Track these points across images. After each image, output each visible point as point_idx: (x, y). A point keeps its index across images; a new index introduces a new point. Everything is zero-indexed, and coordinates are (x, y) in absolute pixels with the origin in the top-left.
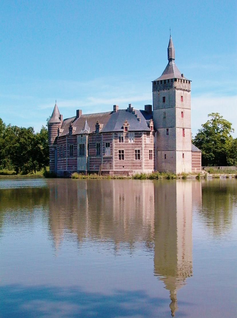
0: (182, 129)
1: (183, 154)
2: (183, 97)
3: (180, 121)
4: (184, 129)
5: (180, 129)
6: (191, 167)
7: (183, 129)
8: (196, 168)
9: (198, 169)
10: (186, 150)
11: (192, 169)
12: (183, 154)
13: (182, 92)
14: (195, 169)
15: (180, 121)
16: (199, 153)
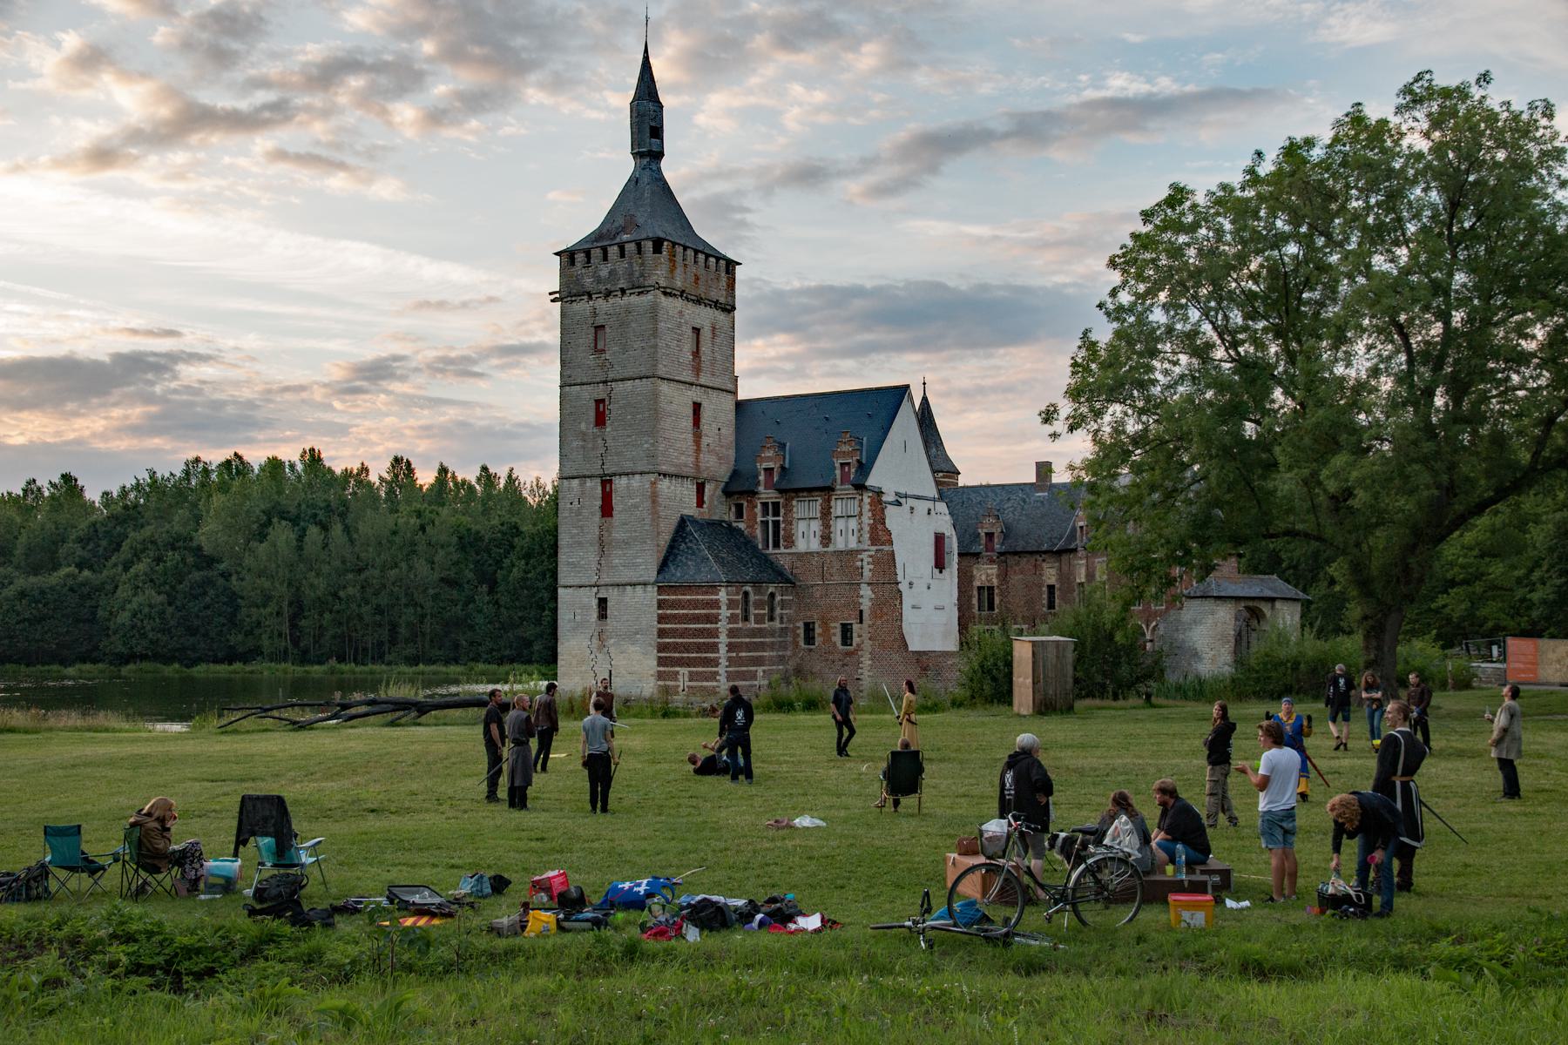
0: (595, 487)
1: (603, 602)
2: (608, 330)
3: (583, 447)
4: (610, 481)
5: (581, 485)
6: (655, 663)
7: (606, 482)
8: (684, 671)
9: (697, 673)
10: (625, 580)
11: (660, 676)
12: (603, 602)
13: (601, 304)
15: (583, 447)
16: (706, 593)
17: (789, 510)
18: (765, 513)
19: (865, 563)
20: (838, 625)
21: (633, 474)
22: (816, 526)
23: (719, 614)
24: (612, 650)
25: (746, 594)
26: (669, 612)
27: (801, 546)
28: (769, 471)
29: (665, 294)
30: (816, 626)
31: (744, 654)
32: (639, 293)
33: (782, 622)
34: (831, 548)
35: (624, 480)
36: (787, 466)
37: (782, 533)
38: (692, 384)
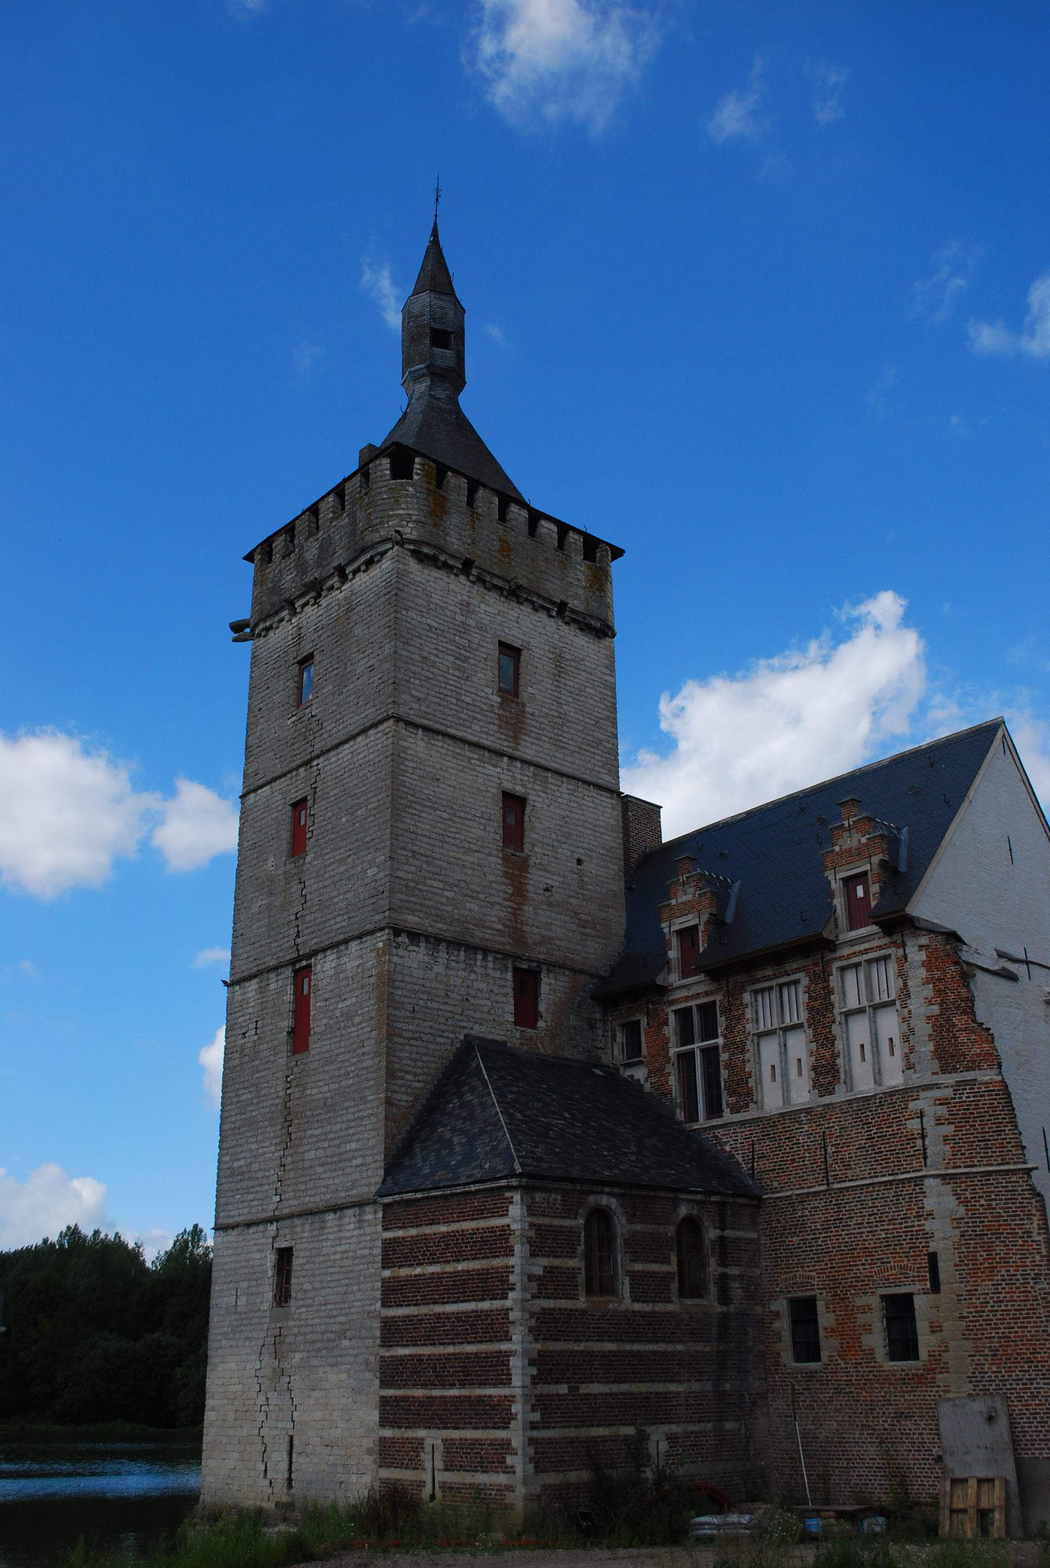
1: (285, 1256)
6: (376, 1416)
8: (432, 1438)
12: (285, 1256)
14: (421, 1442)
15: (269, 907)
16: (479, 1213)
17: (736, 1019)
18: (686, 1037)
19: (929, 1122)
20: (875, 1301)
21: (346, 942)
22: (799, 1045)
23: (509, 1270)
24: (296, 1381)
25: (600, 1216)
26: (404, 1272)
27: (771, 1101)
28: (688, 934)
29: (418, 555)
30: (821, 1306)
31: (597, 1388)
32: (369, 563)
33: (724, 1298)
34: (840, 1096)
35: (331, 956)
36: (729, 918)
37: (724, 1074)
38: (500, 754)
